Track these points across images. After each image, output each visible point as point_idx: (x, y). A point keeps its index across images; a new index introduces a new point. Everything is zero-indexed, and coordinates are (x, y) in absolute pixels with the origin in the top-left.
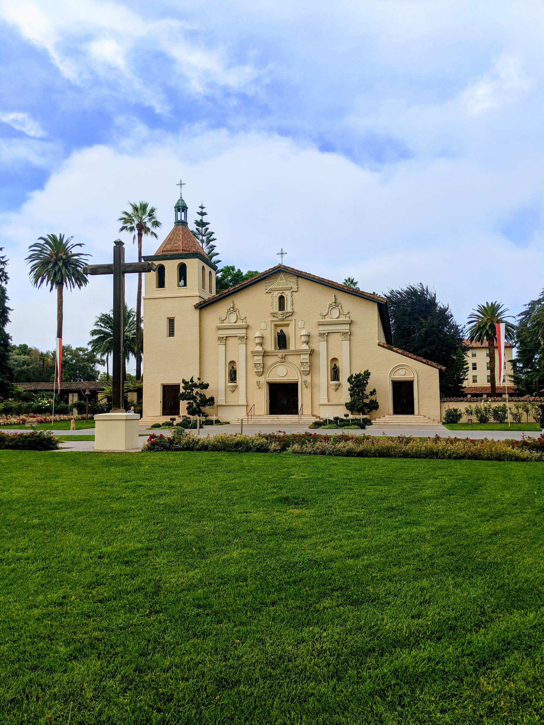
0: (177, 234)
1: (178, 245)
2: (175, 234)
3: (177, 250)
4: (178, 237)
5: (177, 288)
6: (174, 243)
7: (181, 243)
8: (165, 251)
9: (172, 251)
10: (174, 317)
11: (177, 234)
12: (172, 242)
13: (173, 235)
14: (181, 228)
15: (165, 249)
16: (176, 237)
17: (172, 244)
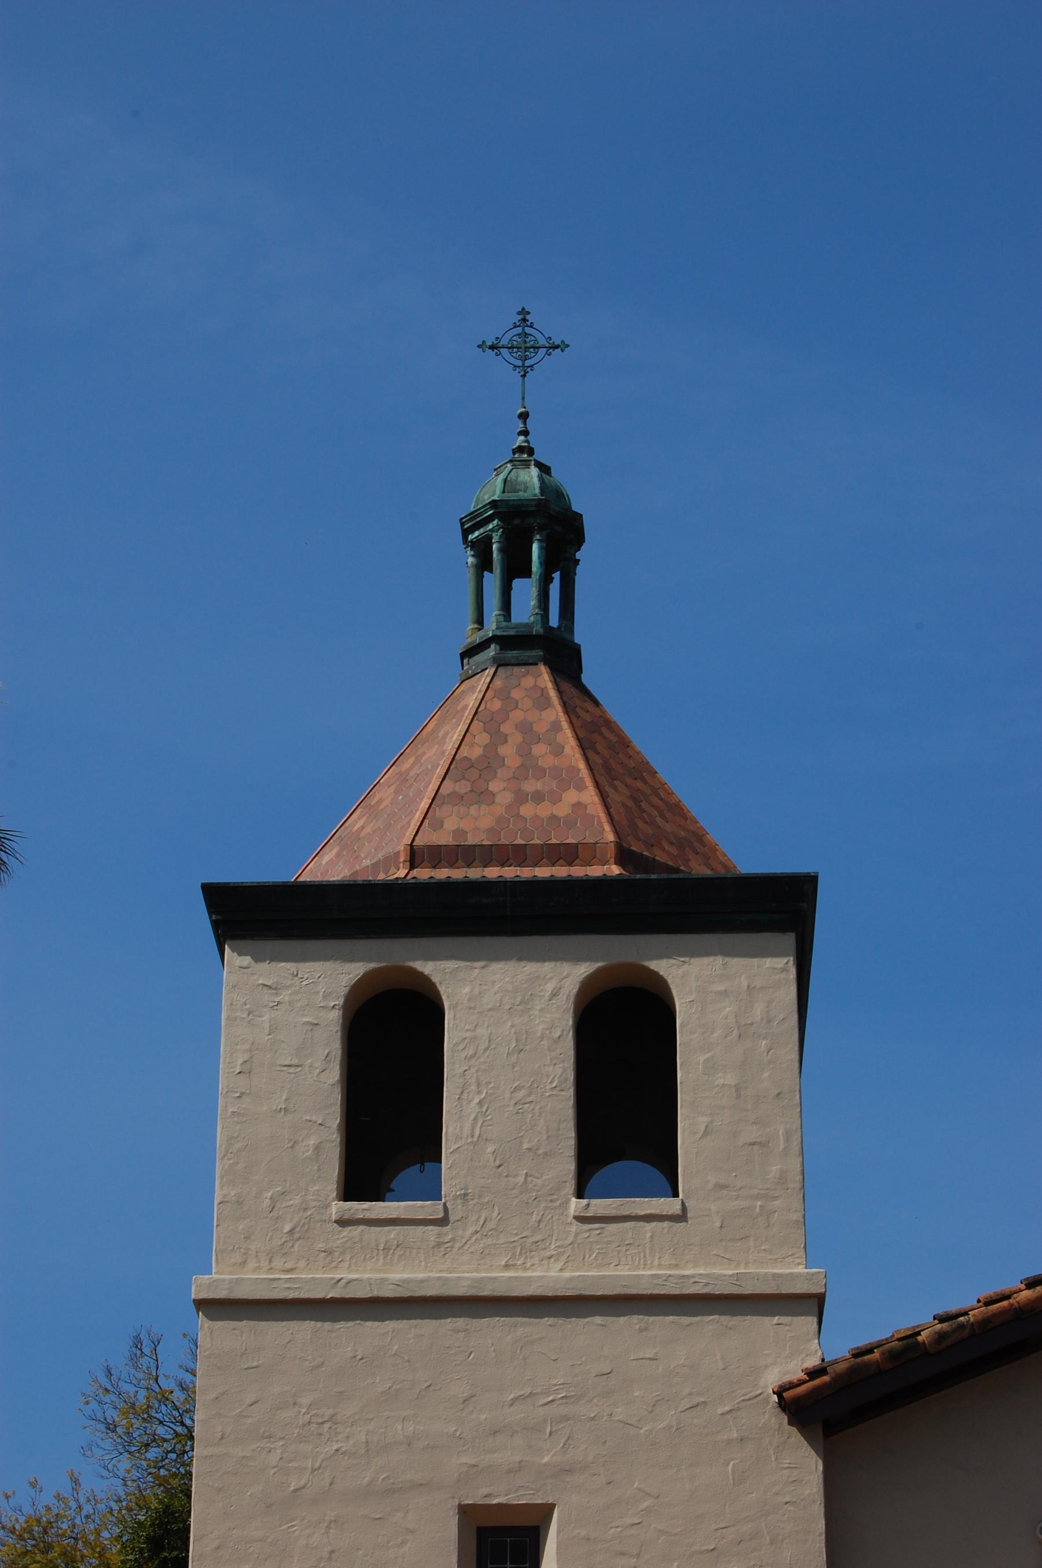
0: (526, 728)
1: (562, 810)
2: (506, 728)
3: (569, 854)
4: (539, 750)
5: (575, 1205)
6: (521, 798)
7: (590, 796)
8: (436, 855)
9: (518, 854)
10: (548, 1510)
11: (526, 728)
12: (494, 786)
13: (483, 738)
14: (550, 685)
15: (443, 838)
16: (524, 751)
17: (504, 798)
